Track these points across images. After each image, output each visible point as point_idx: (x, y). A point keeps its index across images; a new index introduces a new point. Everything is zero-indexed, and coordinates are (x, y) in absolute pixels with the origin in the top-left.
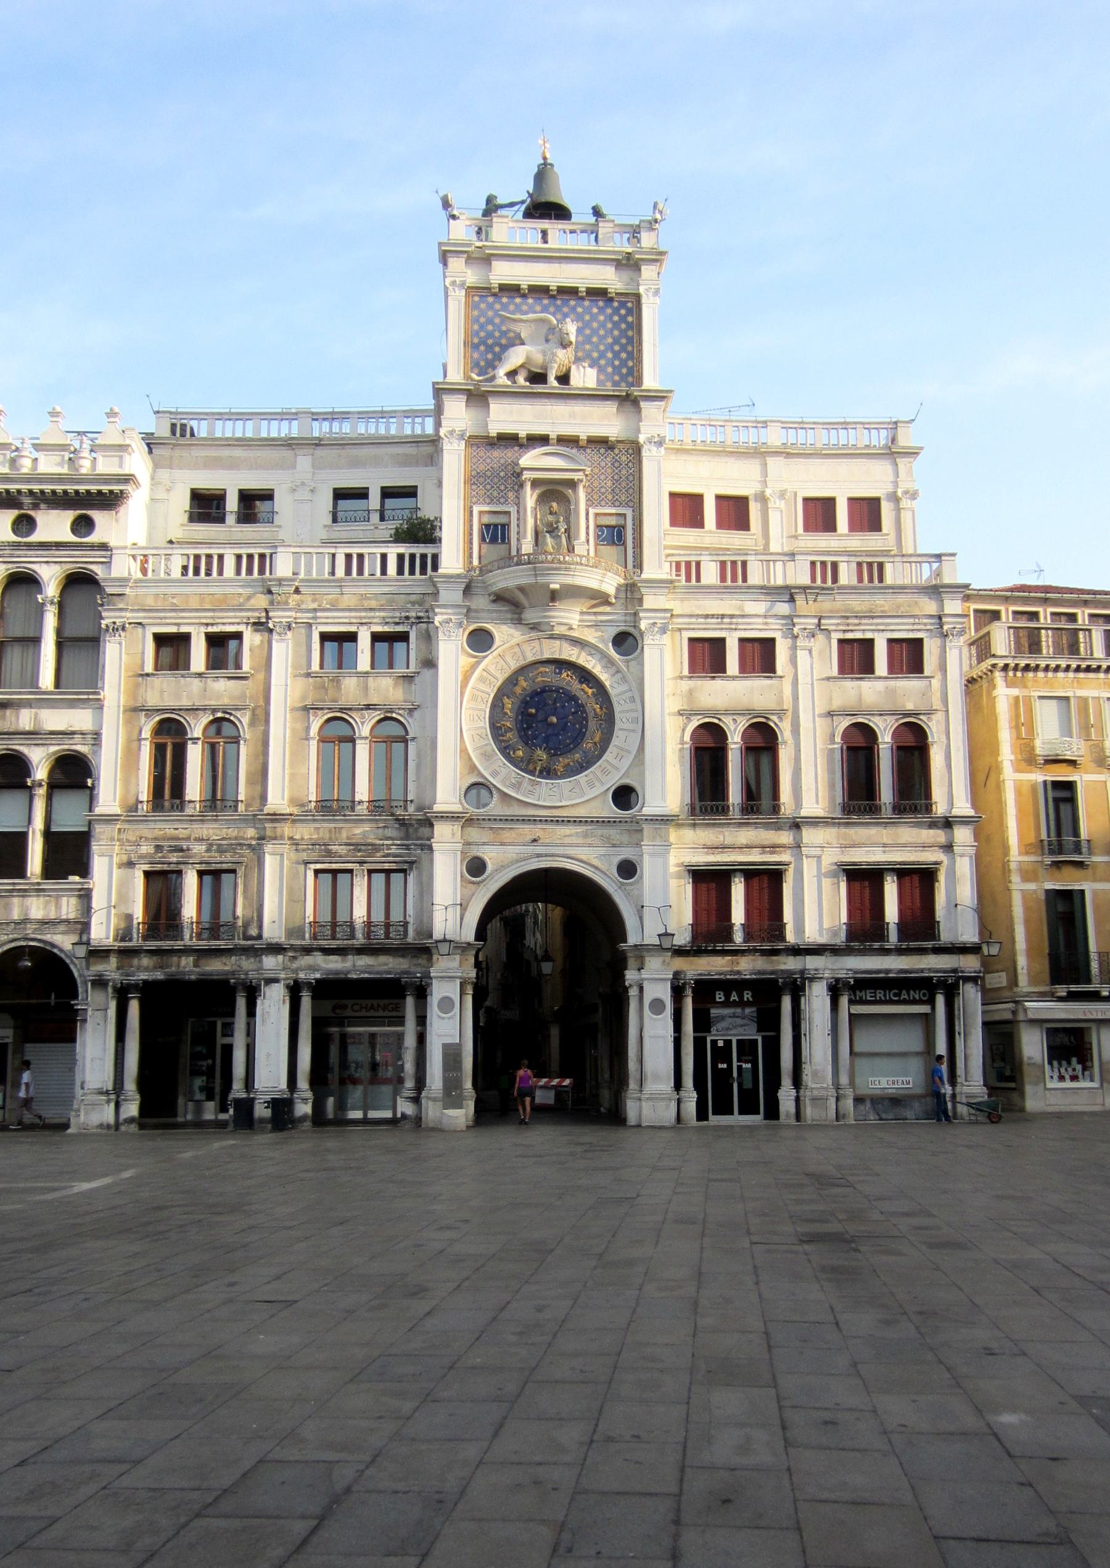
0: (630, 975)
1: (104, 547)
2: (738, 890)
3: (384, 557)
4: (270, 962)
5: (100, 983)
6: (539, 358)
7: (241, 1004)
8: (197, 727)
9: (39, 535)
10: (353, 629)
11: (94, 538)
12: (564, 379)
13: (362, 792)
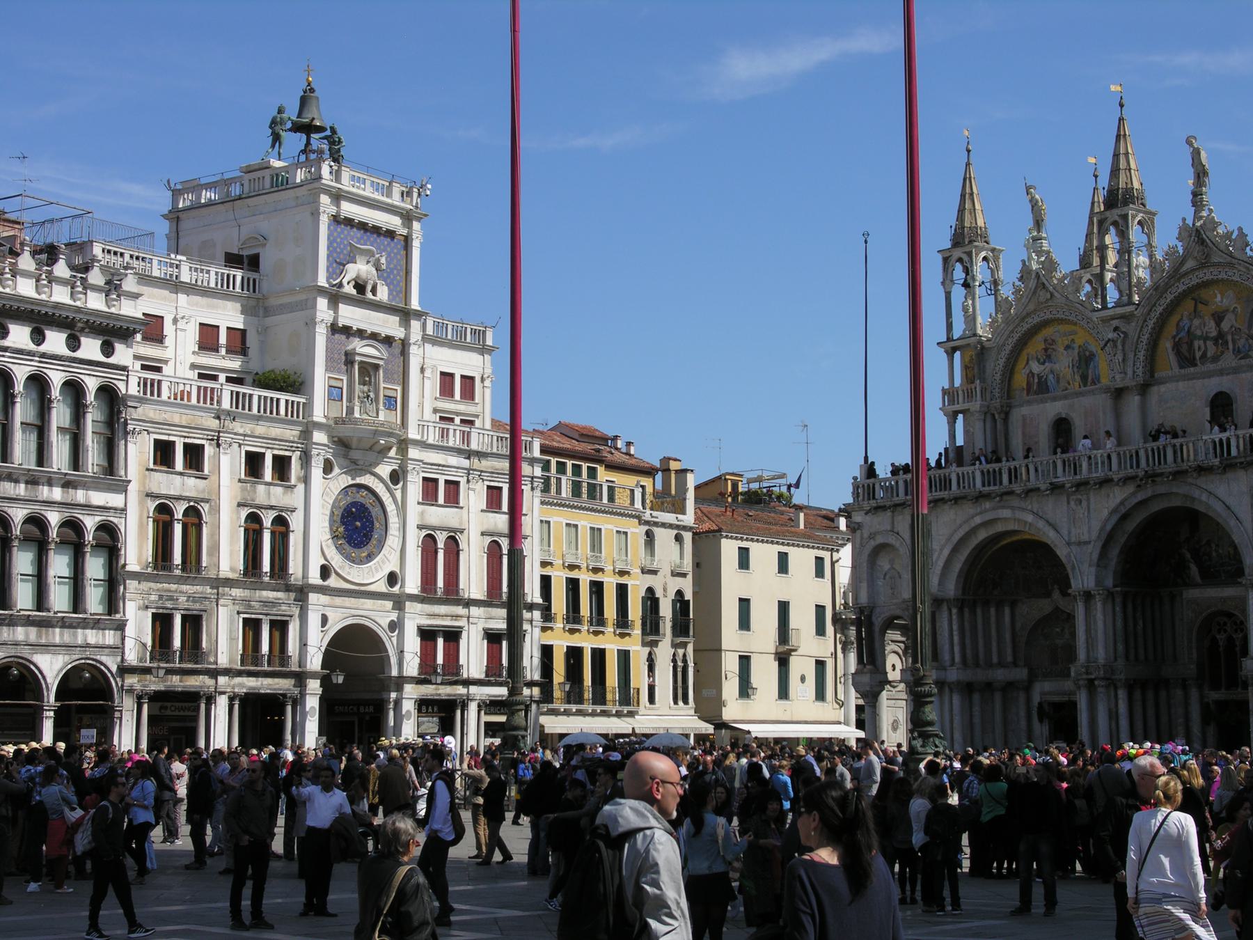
0: (393, 695)
1: (124, 368)
2: (440, 641)
3: (278, 400)
4: (222, 680)
5: (130, 691)
6: (364, 275)
7: (203, 706)
8: (179, 510)
9: (79, 354)
10: (262, 450)
11: (111, 360)
12: (374, 291)
13: (266, 566)
